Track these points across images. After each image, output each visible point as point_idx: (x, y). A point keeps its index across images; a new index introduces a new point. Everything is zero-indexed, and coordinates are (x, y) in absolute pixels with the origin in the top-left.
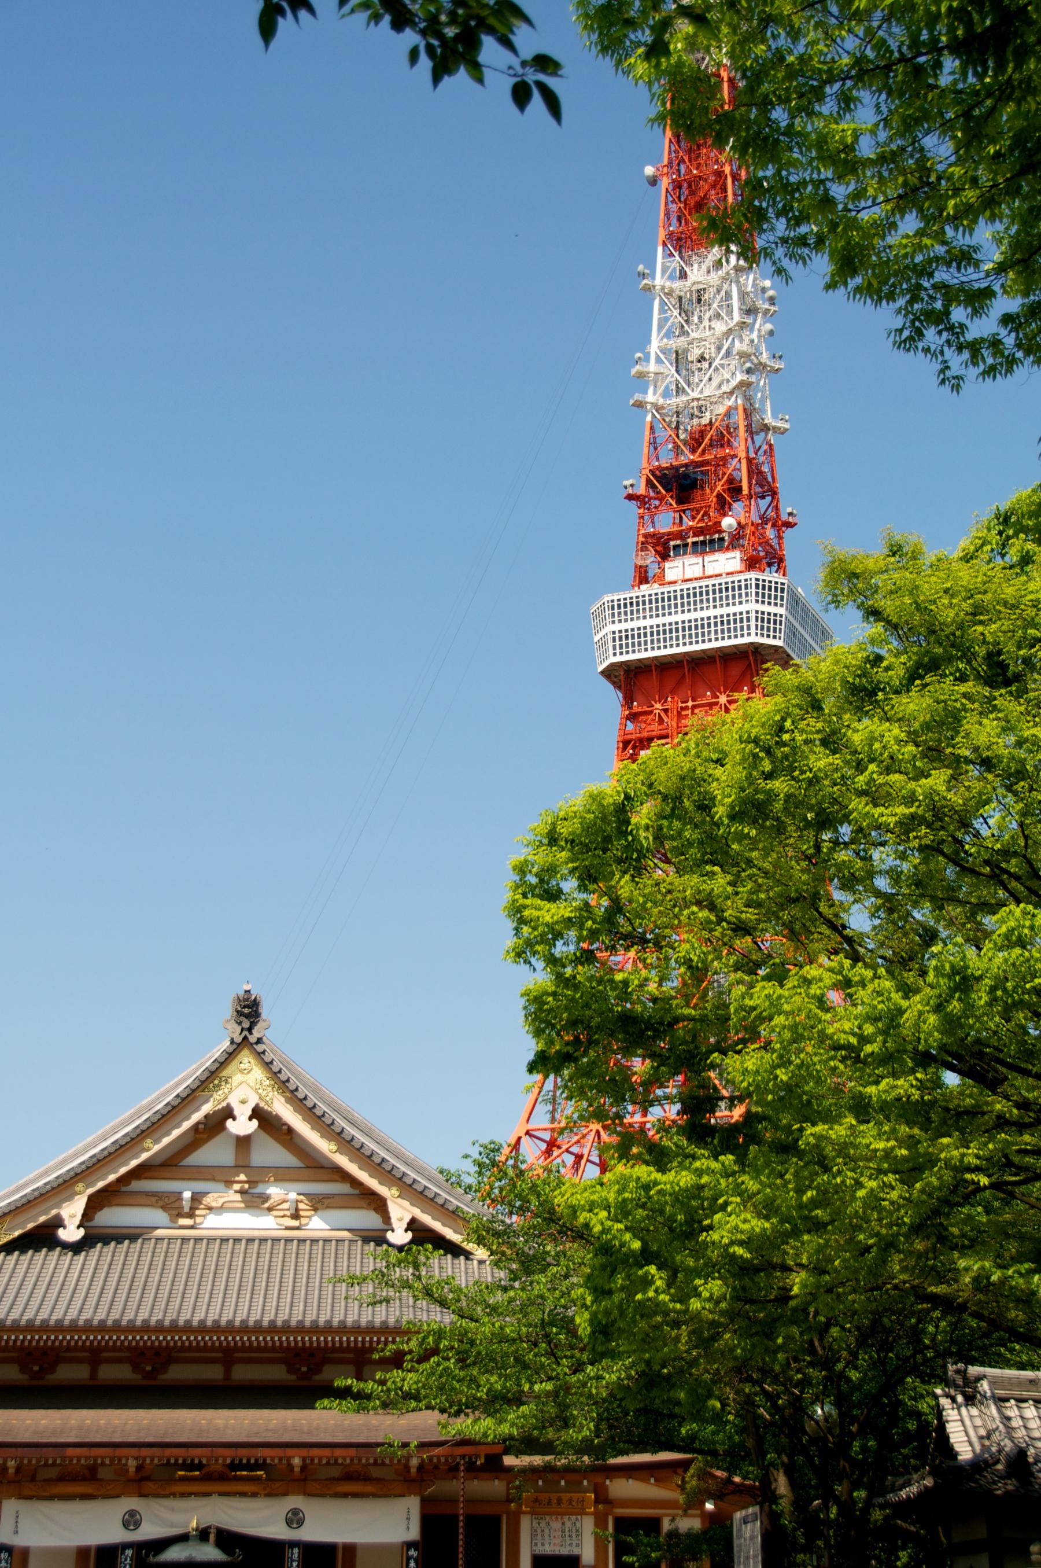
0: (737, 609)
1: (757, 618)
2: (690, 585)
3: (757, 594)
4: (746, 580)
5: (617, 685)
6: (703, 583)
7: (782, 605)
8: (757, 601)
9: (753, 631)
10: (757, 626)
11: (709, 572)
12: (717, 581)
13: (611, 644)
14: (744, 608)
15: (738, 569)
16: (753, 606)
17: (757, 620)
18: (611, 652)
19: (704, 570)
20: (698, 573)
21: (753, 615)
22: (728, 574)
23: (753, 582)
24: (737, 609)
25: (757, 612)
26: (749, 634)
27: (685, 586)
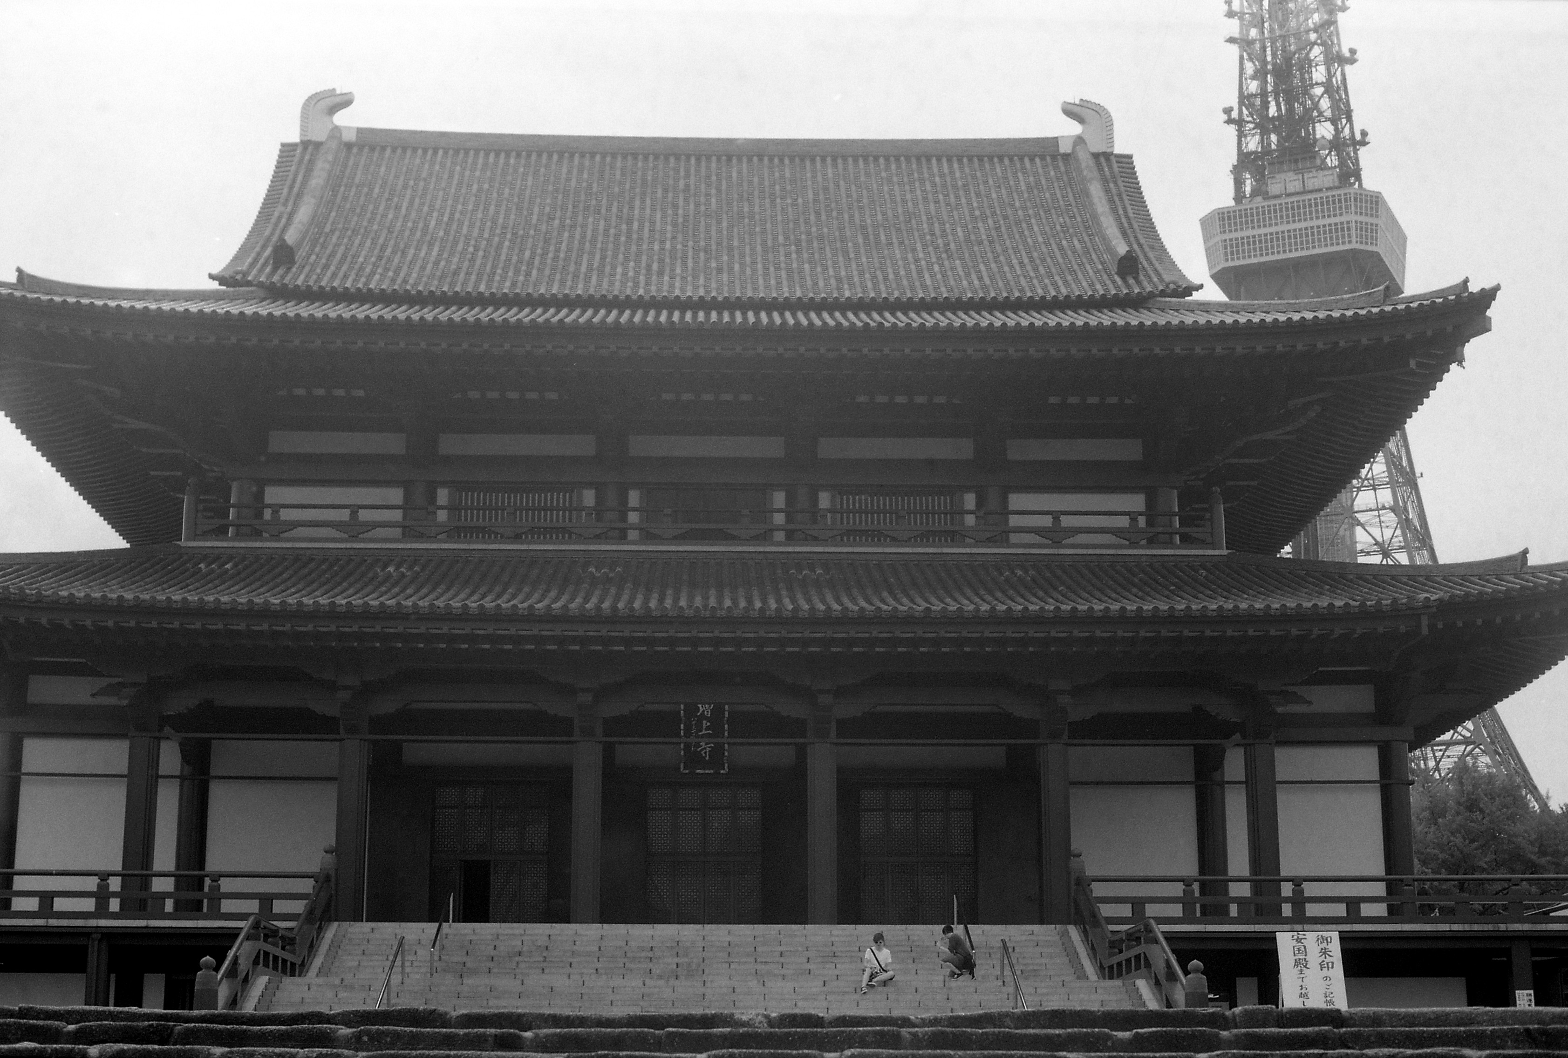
0: (1338, 219)
1: (1356, 227)
4: (1345, 194)
6: (1307, 197)
7: (1377, 216)
8: (1356, 213)
9: (1354, 238)
10: (1357, 235)
12: (1318, 195)
14: (1344, 219)
15: (1337, 184)
16: (1353, 218)
17: (1356, 230)
18: (1223, 258)
19: (1304, 185)
22: (1328, 189)
25: (1356, 222)
26: (1350, 242)
27: (1290, 200)
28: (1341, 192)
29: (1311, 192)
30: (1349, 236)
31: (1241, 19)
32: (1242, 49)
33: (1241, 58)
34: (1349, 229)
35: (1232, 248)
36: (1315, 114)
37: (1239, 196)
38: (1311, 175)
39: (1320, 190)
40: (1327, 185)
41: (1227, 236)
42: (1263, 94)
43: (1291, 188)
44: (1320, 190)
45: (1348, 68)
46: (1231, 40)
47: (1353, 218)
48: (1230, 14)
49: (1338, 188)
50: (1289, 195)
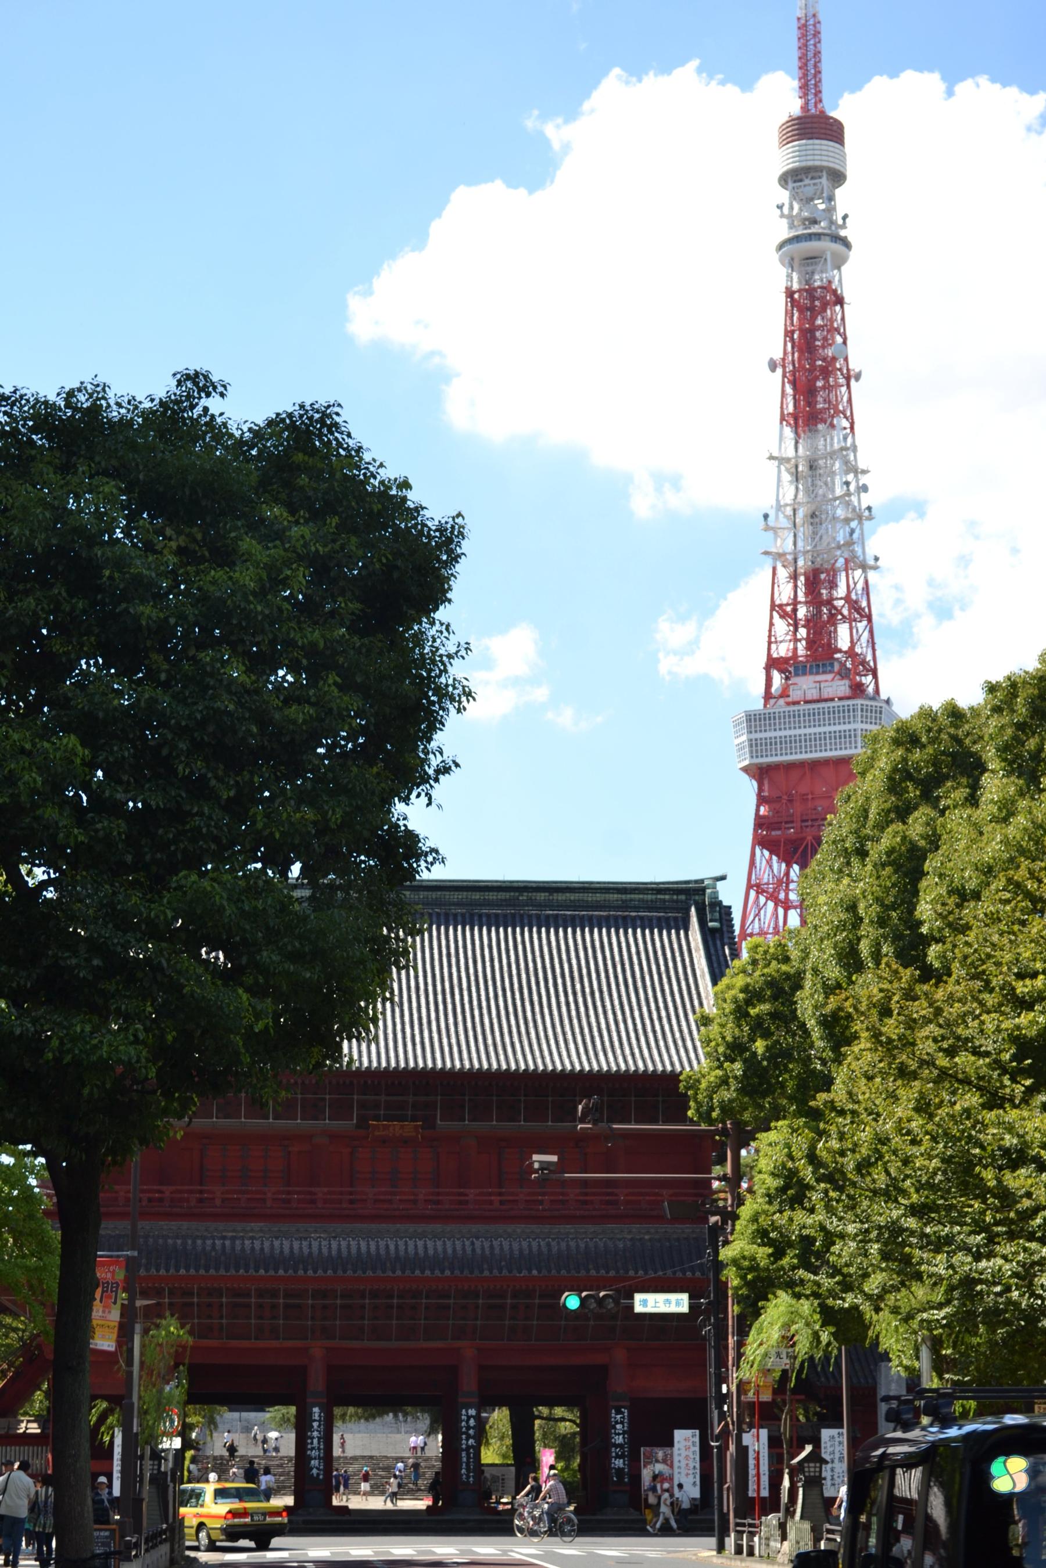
0: (847, 727)
2: (811, 706)
3: (862, 716)
5: (753, 776)
11: (825, 695)
13: (747, 750)
14: (852, 726)
16: (859, 726)
18: (748, 756)
20: (816, 696)
21: (859, 732)
22: (840, 699)
23: (859, 707)
24: (847, 727)
26: (856, 747)
28: (850, 702)
29: (826, 700)
30: (856, 742)
31: (776, 533)
32: (775, 560)
33: (774, 569)
34: (855, 736)
35: (754, 746)
36: (840, 617)
37: (768, 696)
38: (827, 684)
39: (832, 700)
40: (841, 694)
41: (754, 736)
42: (795, 603)
43: (809, 697)
44: (832, 700)
45: (872, 575)
46: (766, 553)
47: (859, 726)
48: (767, 528)
49: (848, 698)
50: (807, 702)
